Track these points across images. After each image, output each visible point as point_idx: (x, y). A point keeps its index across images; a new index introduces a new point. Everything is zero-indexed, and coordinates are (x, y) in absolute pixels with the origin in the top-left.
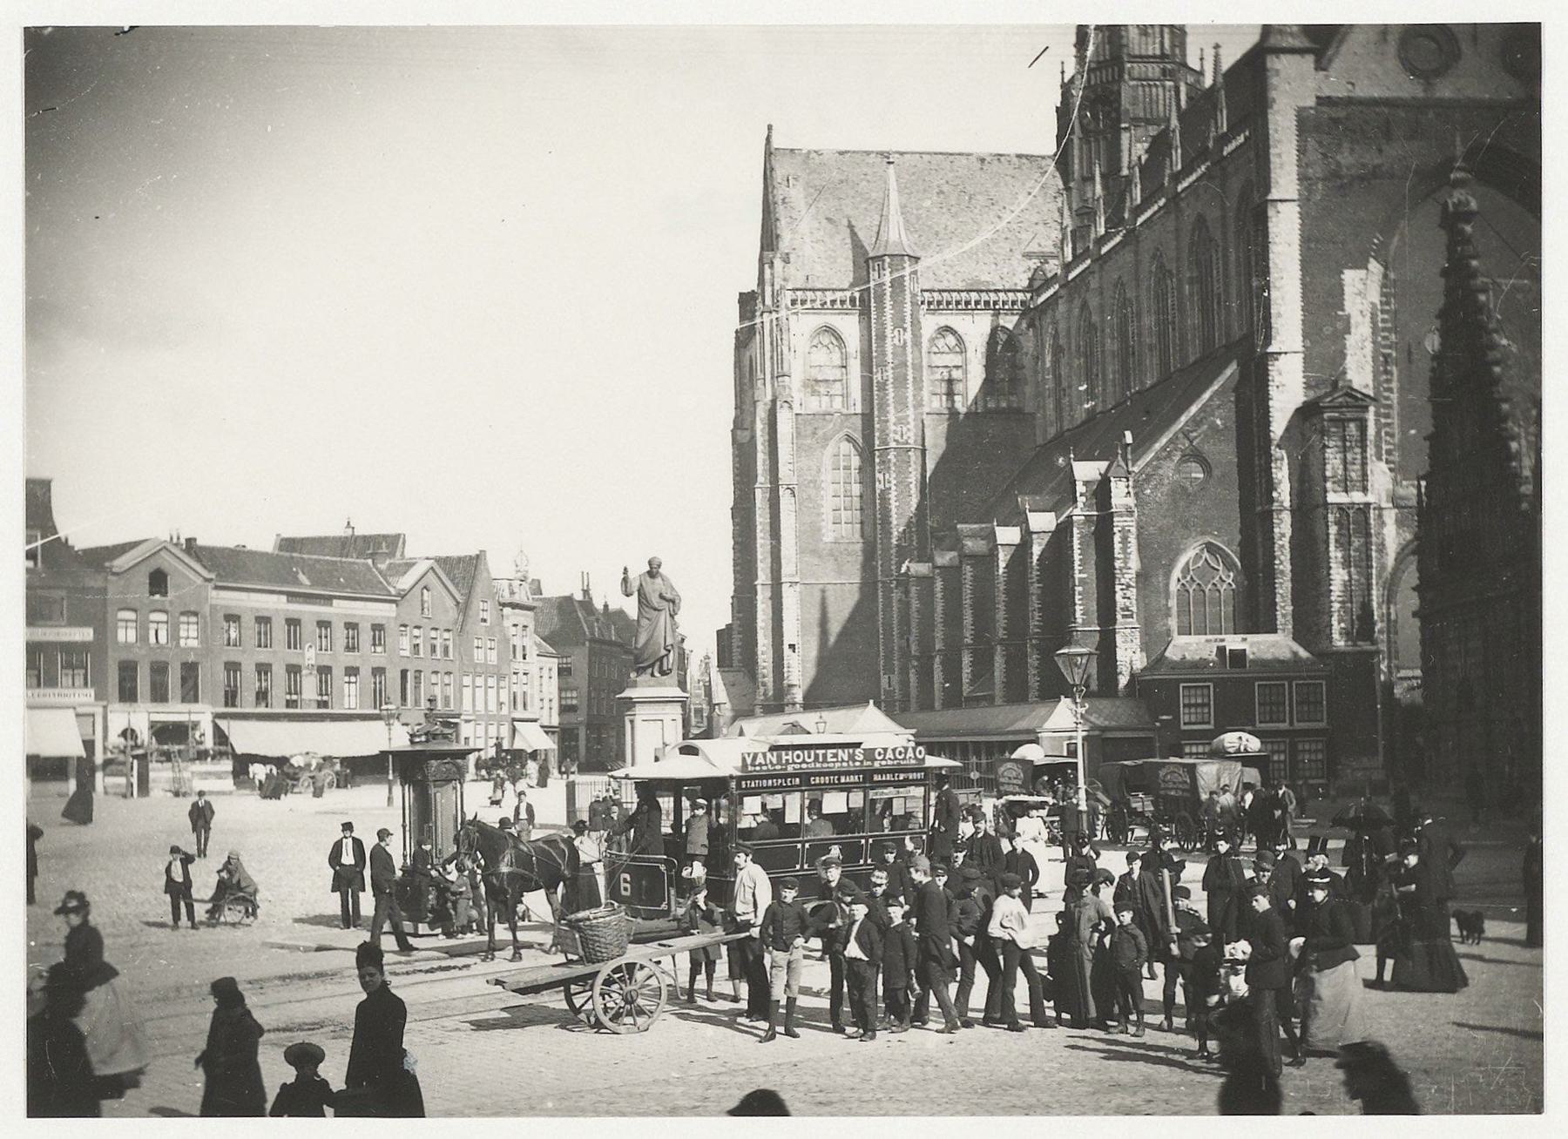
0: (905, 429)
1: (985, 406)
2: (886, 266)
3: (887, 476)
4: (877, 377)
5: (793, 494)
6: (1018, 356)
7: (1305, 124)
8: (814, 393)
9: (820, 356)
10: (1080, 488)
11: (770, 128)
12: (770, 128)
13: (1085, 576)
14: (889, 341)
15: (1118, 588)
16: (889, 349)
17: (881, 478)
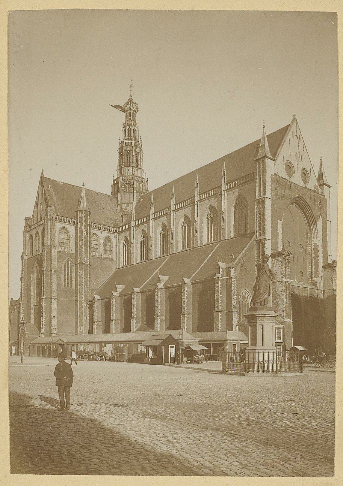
0: (87, 259)
1: (103, 256)
2: (84, 213)
3: (82, 271)
4: (79, 243)
5: (56, 273)
6: (111, 244)
7: (272, 180)
8: (60, 246)
9: (62, 236)
10: (221, 270)
11: (43, 170)
12: (43, 170)
13: (221, 295)
14: (83, 234)
15: (233, 299)
16: (84, 236)
17: (80, 271)
